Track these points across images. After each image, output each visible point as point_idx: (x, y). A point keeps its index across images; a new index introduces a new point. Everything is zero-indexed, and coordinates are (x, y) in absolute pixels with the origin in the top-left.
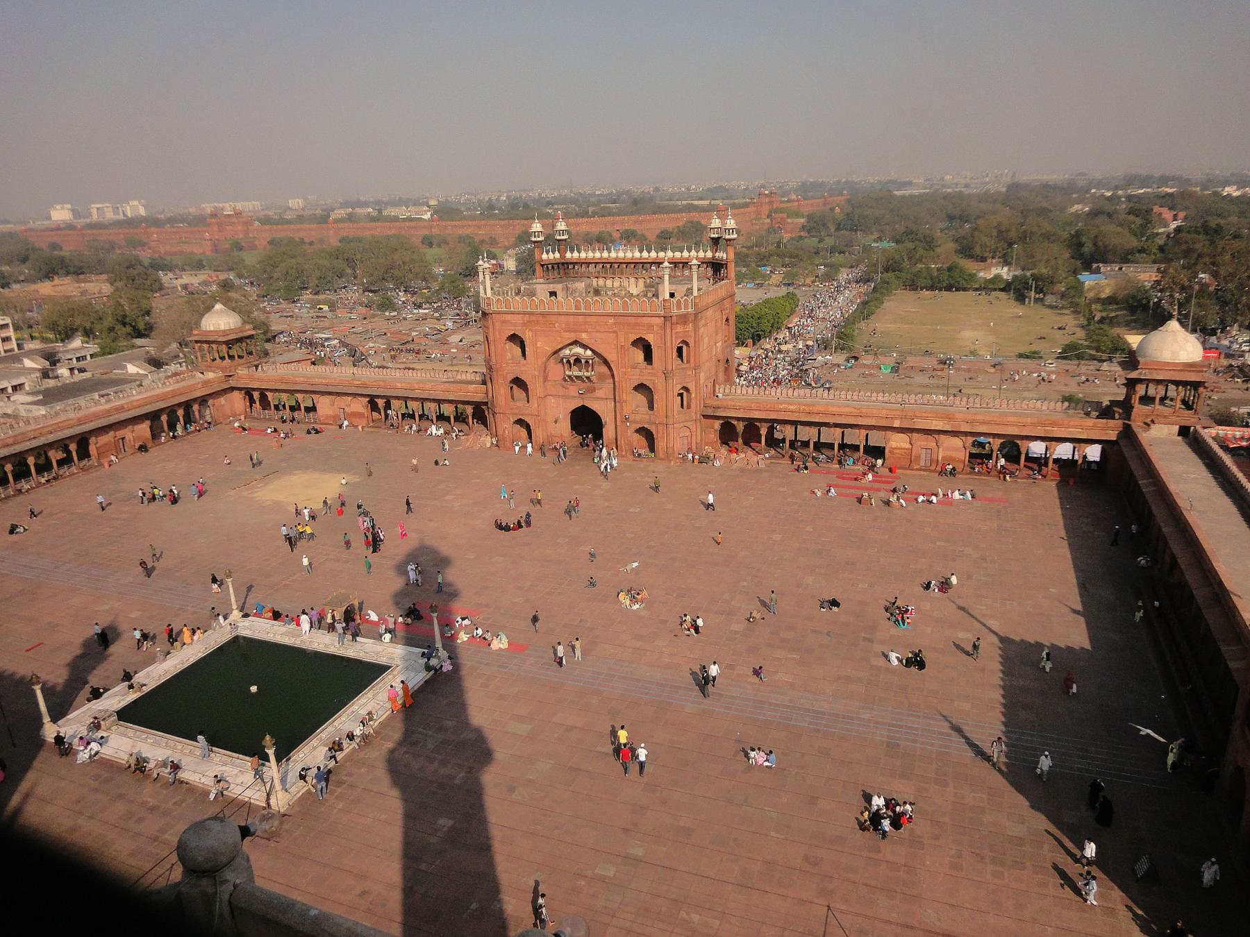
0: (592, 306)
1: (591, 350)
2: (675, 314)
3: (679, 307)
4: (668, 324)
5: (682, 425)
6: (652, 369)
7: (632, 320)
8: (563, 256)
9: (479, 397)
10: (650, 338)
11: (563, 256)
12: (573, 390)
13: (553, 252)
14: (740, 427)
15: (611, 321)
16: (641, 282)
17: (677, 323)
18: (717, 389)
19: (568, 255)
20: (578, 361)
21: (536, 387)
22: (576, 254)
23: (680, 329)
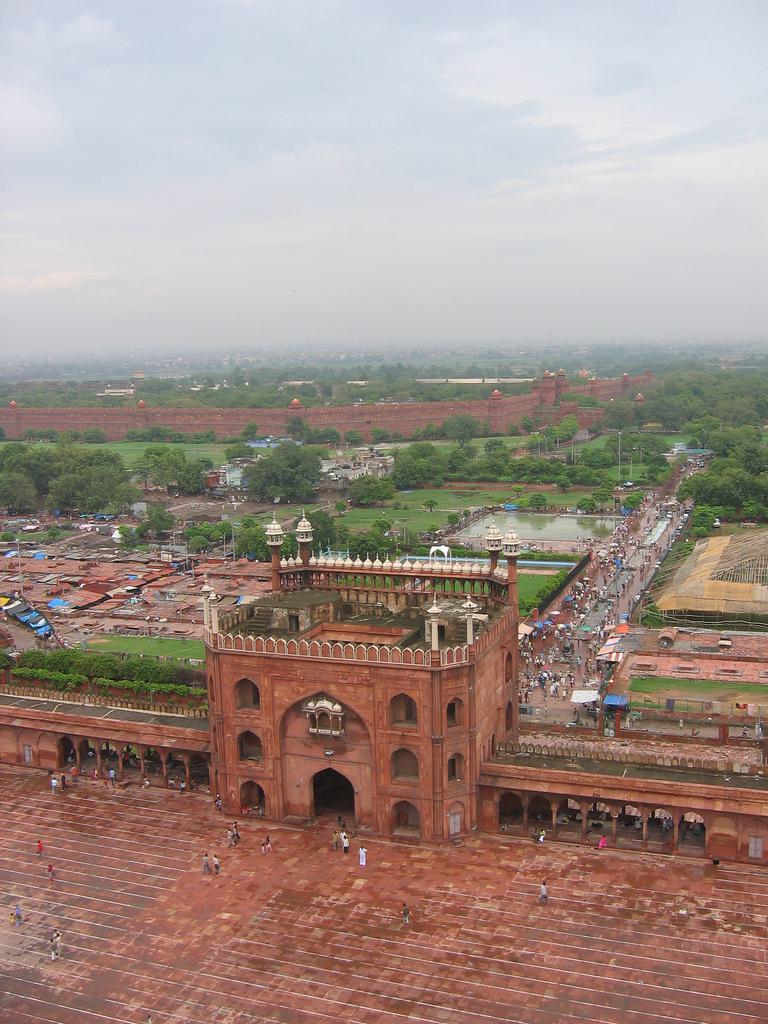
0: (343, 653)
1: (340, 704)
3: (450, 660)
4: (437, 680)
5: (453, 800)
7: (392, 673)
8: (306, 563)
9: (197, 747)
10: (415, 695)
12: (317, 752)
14: (525, 803)
17: (448, 679)
19: (313, 560)
20: (324, 714)
21: (271, 748)
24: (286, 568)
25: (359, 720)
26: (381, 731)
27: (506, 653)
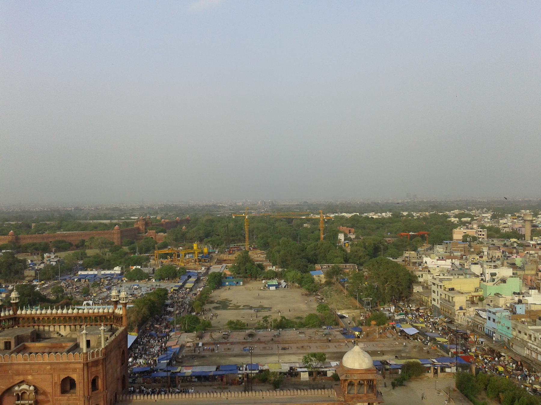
1: (33, 386)
2: (91, 361)
3: (93, 356)
6: (76, 396)
8: (15, 313)
10: (74, 377)
11: (15, 313)
13: (9, 311)
15: (49, 367)
16: (68, 328)
17: (92, 366)
18: (118, 397)
19: (19, 312)
22: (24, 312)
23: (94, 369)
24: (3, 317)
25: (44, 393)
26: (56, 398)
27: (122, 350)
